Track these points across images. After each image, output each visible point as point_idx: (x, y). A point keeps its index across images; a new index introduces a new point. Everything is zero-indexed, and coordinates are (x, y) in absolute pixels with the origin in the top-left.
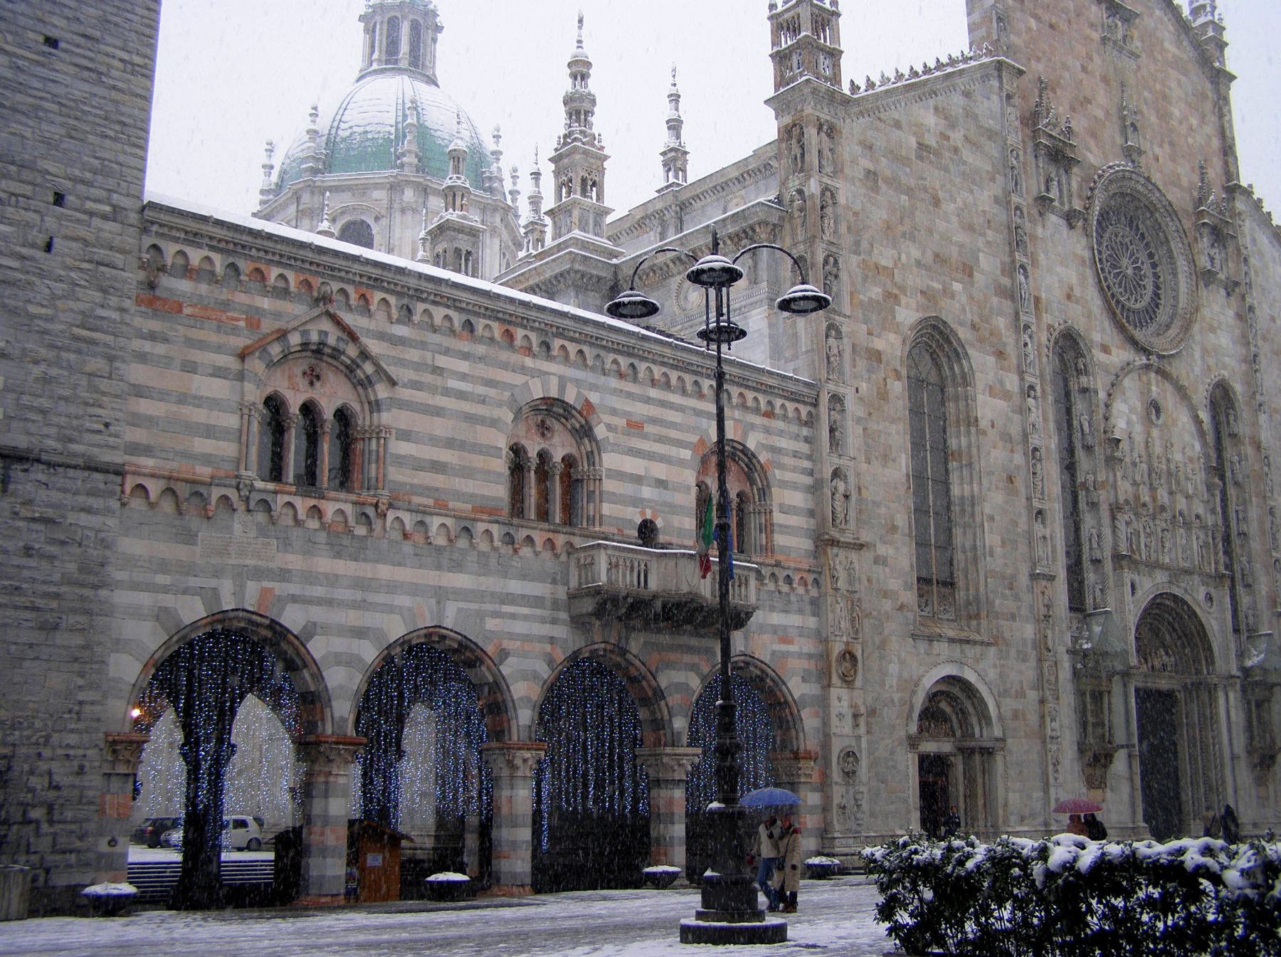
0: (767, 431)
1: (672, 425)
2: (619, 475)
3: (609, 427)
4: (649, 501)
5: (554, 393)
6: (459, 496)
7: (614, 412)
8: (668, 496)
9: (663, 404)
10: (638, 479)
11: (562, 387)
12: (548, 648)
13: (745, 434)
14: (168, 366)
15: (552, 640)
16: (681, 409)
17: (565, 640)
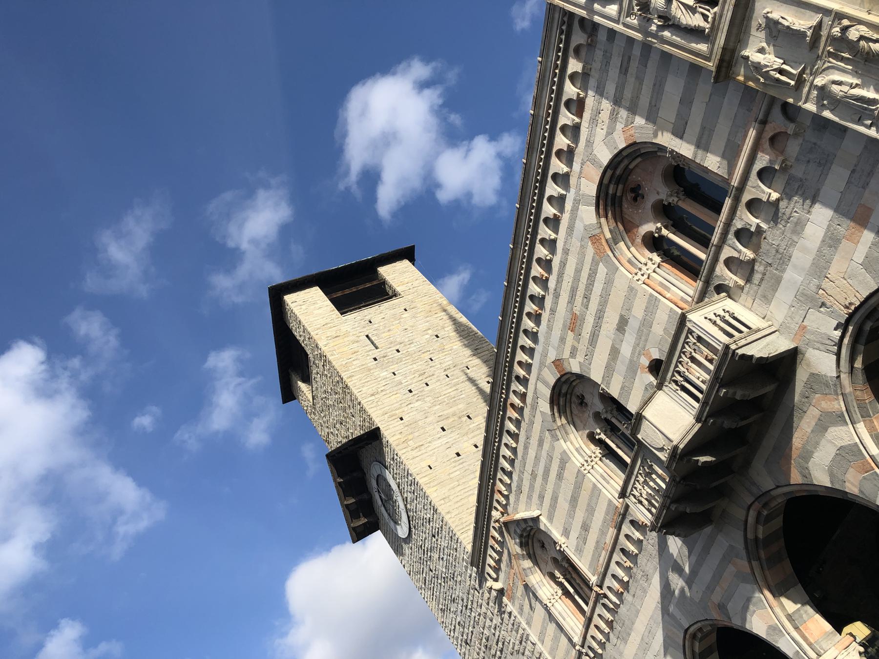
0: (594, 121)
1: (578, 271)
2: (609, 370)
3: (573, 354)
4: (633, 353)
5: (547, 392)
6: (603, 533)
7: (563, 340)
8: (633, 325)
9: (561, 275)
10: (615, 352)
11: (545, 383)
12: (731, 569)
13: (595, 162)
14: (532, 617)
15: (726, 559)
16: (566, 252)
17: (731, 546)
